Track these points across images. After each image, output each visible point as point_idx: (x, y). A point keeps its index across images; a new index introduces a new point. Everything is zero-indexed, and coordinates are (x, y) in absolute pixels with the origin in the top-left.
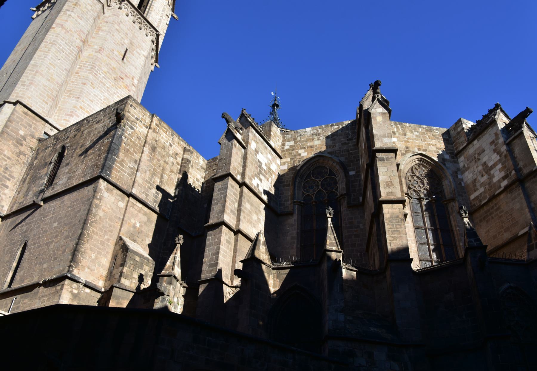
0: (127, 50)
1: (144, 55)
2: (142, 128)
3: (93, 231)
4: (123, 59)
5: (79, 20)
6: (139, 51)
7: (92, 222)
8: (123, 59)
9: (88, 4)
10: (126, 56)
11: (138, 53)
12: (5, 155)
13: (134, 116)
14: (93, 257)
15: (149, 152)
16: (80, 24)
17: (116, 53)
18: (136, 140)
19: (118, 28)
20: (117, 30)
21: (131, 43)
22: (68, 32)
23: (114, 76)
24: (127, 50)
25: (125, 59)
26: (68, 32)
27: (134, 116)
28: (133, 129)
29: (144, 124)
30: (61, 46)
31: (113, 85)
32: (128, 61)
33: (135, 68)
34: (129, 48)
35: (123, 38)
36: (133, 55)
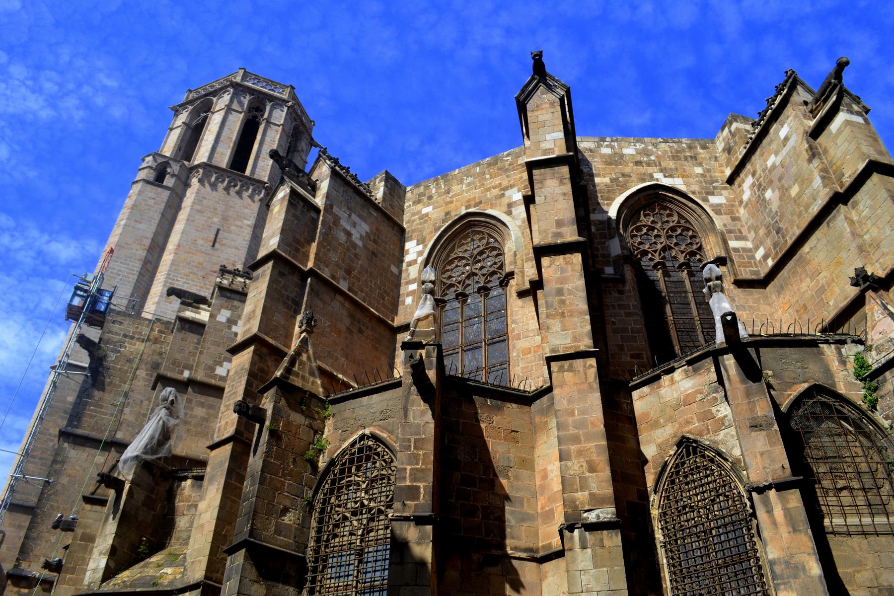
0: (218, 230)
1: (248, 226)
2: (135, 344)
3: (52, 506)
4: (213, 246)
5: (138, 226)
6: (240, 223)
7: (50, 495)
8: (213, 246)
9: (150, 198)
10: (218, 240)
11: (236, 226)
12: (50, 435)
13: (119, 335)
14: (53, 541)
15: (147, 375)
16: (139, 229)
17: (200, 242)
18: (123, 365)
19: (199, 208)
20: (199, 211)
21: (225, 219)
22: (123, 247)
23: (201, 273)
24: (218, 230)
25: (217, 245)
26: (123, 247)
27: (119, 335)
28: (119, 352)
29: (138, 339)
30: (114, 269)
31: (201, 287)
32: (224, 245)
33: (236, 248)
34: (223, 226)
35: (209, 218)
36: (230, 232)
